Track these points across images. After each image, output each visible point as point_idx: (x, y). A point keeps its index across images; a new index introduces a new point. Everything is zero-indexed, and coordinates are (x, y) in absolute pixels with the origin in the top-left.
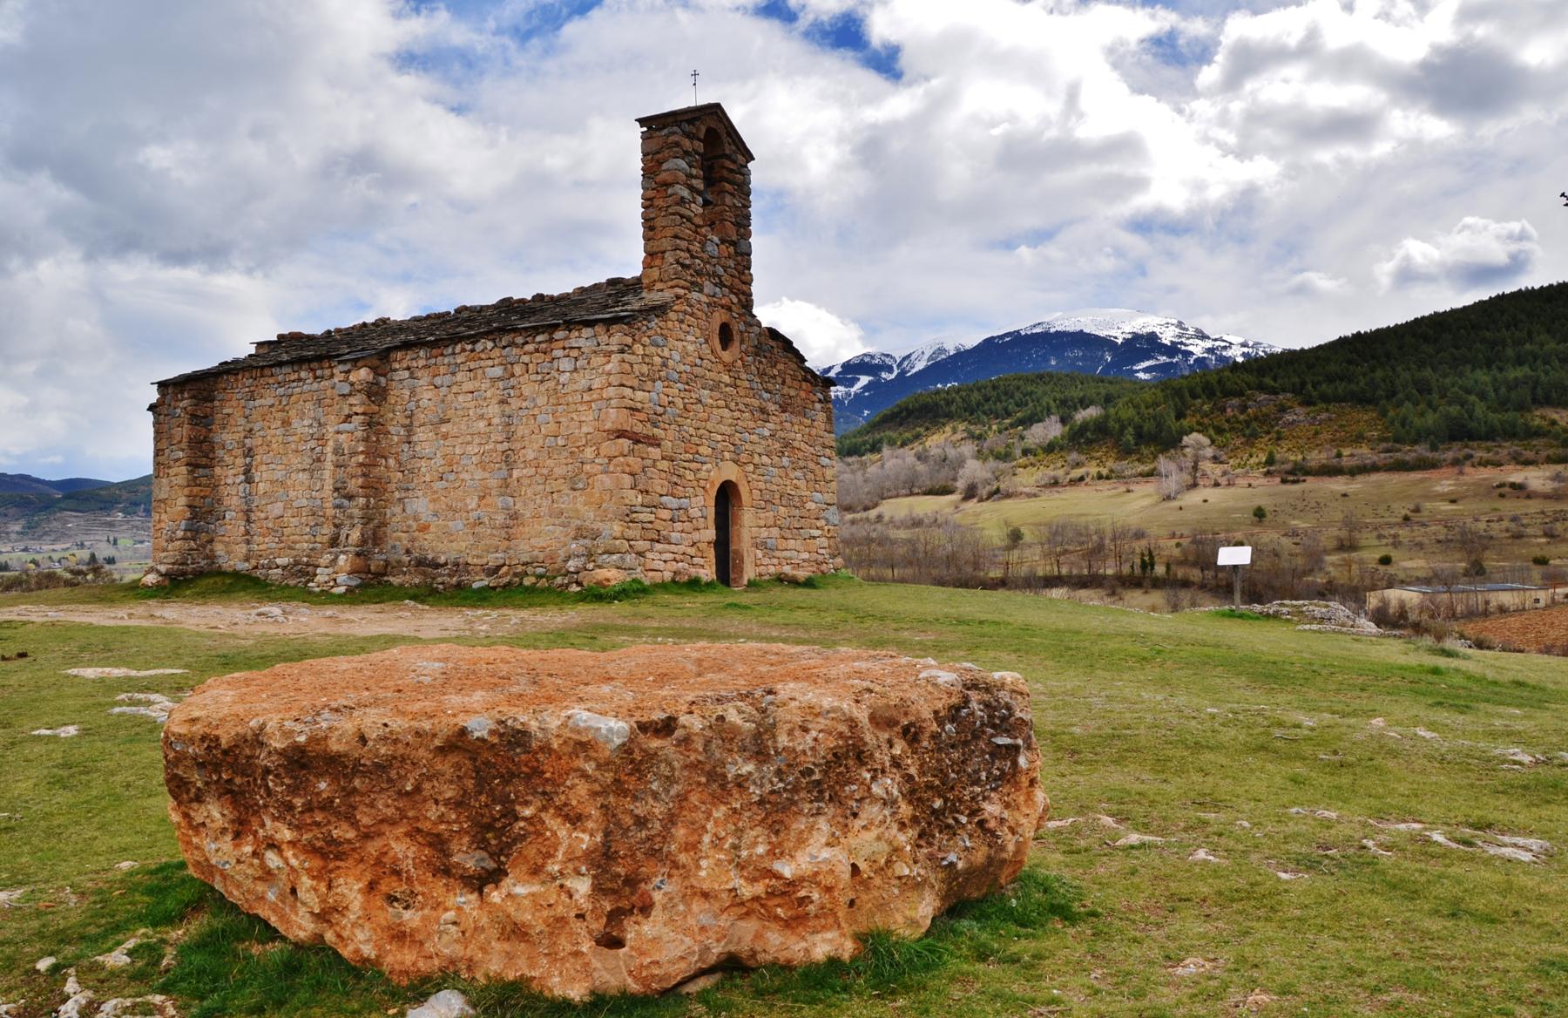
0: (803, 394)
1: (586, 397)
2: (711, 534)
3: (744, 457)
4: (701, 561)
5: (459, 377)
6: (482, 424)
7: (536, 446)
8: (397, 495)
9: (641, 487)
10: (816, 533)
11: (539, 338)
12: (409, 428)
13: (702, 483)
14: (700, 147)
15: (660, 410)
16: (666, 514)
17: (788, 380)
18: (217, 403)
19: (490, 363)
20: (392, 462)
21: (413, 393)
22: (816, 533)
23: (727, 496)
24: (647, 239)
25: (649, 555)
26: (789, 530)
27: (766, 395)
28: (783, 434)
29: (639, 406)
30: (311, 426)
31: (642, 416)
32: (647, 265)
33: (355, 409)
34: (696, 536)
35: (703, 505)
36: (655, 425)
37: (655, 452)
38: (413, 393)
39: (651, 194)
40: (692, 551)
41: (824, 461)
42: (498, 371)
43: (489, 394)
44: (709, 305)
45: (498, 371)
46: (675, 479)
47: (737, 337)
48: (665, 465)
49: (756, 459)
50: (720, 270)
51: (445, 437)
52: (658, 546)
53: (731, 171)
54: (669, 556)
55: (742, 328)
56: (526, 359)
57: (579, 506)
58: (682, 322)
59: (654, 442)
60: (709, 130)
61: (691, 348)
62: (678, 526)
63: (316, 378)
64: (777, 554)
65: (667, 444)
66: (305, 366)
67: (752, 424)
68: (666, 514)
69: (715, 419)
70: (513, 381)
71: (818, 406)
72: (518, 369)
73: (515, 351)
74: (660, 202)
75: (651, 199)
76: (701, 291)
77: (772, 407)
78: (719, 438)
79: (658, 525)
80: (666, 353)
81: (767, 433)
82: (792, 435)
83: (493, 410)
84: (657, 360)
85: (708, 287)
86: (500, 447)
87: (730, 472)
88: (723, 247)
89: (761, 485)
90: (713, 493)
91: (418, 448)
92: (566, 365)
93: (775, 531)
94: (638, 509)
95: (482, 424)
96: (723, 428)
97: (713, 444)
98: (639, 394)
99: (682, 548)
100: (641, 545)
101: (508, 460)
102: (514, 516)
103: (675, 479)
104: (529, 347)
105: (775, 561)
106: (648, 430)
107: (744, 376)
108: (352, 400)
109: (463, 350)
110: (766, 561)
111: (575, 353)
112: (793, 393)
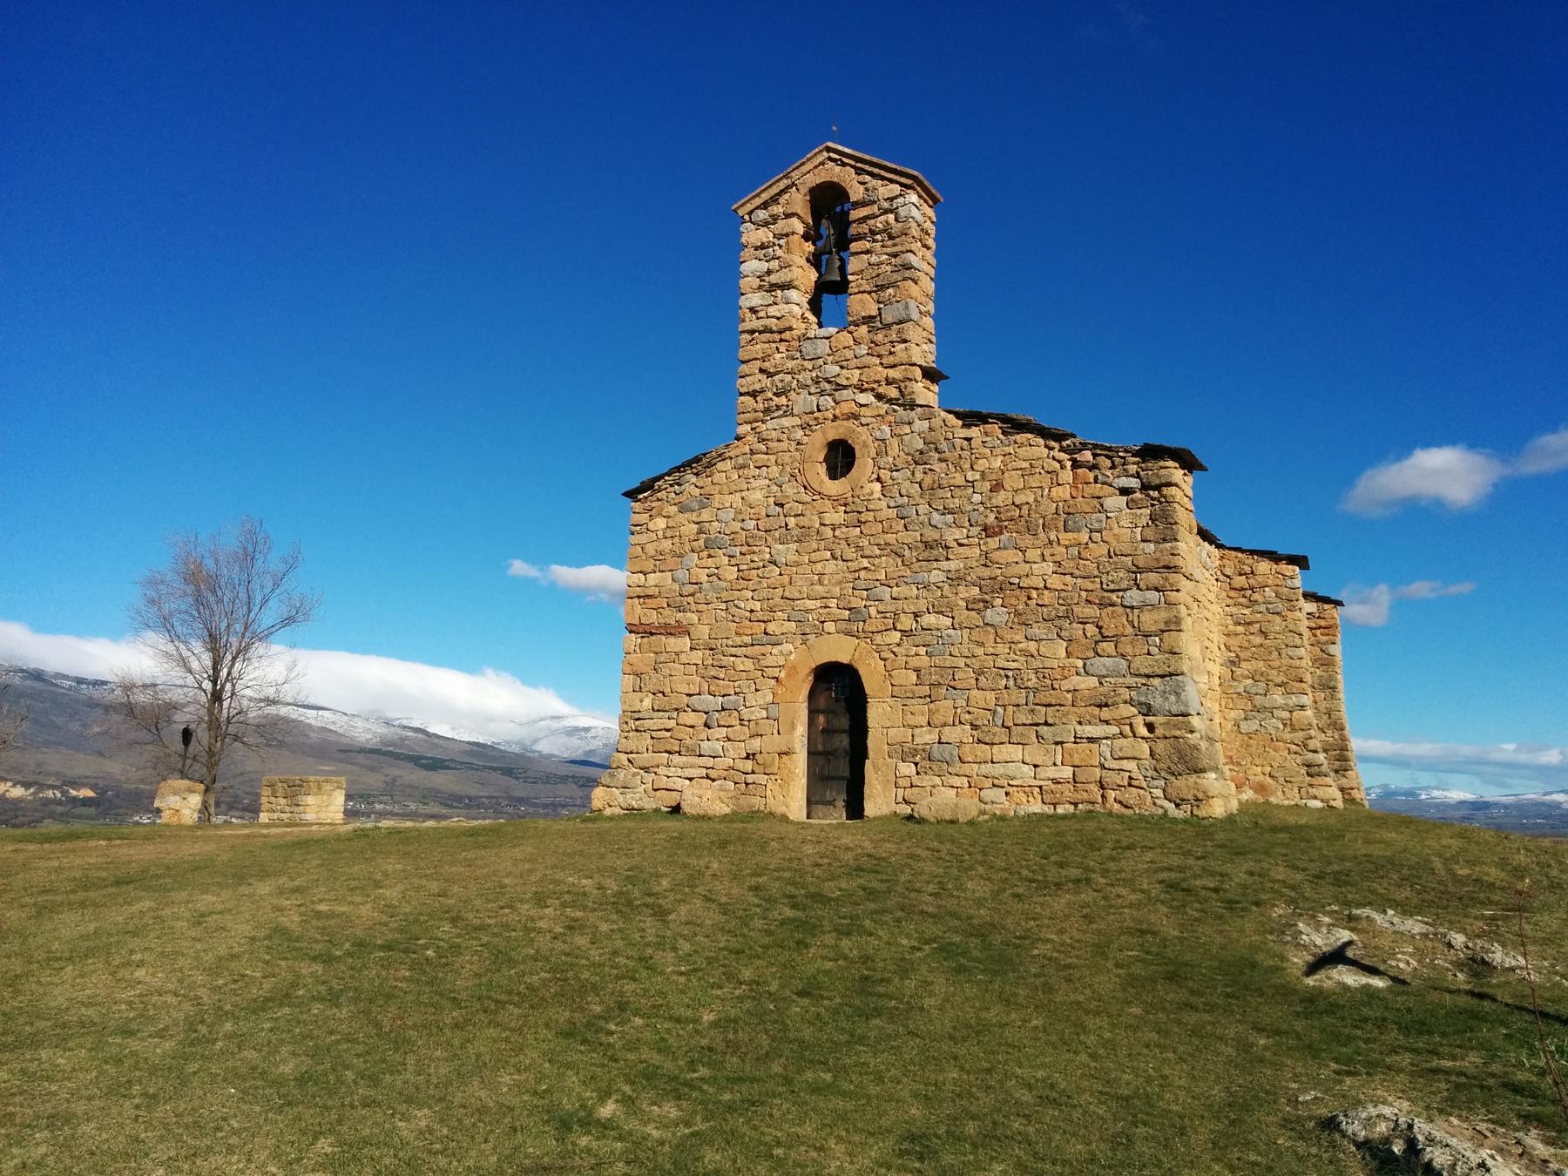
9: (652, 688)
16: (698, 719)
34: (756, 744)
36: (680, 609)
37: (674, 643)
49: (906, 622)
52: (676, 759)
58: (743, 467)
59: (679, 630)
61: (757, 496)
65: (703, 632)
76: (788, 413)
78: (810, 604)
87: (839, 650)
89: (924, 661)
106: (671, 617)
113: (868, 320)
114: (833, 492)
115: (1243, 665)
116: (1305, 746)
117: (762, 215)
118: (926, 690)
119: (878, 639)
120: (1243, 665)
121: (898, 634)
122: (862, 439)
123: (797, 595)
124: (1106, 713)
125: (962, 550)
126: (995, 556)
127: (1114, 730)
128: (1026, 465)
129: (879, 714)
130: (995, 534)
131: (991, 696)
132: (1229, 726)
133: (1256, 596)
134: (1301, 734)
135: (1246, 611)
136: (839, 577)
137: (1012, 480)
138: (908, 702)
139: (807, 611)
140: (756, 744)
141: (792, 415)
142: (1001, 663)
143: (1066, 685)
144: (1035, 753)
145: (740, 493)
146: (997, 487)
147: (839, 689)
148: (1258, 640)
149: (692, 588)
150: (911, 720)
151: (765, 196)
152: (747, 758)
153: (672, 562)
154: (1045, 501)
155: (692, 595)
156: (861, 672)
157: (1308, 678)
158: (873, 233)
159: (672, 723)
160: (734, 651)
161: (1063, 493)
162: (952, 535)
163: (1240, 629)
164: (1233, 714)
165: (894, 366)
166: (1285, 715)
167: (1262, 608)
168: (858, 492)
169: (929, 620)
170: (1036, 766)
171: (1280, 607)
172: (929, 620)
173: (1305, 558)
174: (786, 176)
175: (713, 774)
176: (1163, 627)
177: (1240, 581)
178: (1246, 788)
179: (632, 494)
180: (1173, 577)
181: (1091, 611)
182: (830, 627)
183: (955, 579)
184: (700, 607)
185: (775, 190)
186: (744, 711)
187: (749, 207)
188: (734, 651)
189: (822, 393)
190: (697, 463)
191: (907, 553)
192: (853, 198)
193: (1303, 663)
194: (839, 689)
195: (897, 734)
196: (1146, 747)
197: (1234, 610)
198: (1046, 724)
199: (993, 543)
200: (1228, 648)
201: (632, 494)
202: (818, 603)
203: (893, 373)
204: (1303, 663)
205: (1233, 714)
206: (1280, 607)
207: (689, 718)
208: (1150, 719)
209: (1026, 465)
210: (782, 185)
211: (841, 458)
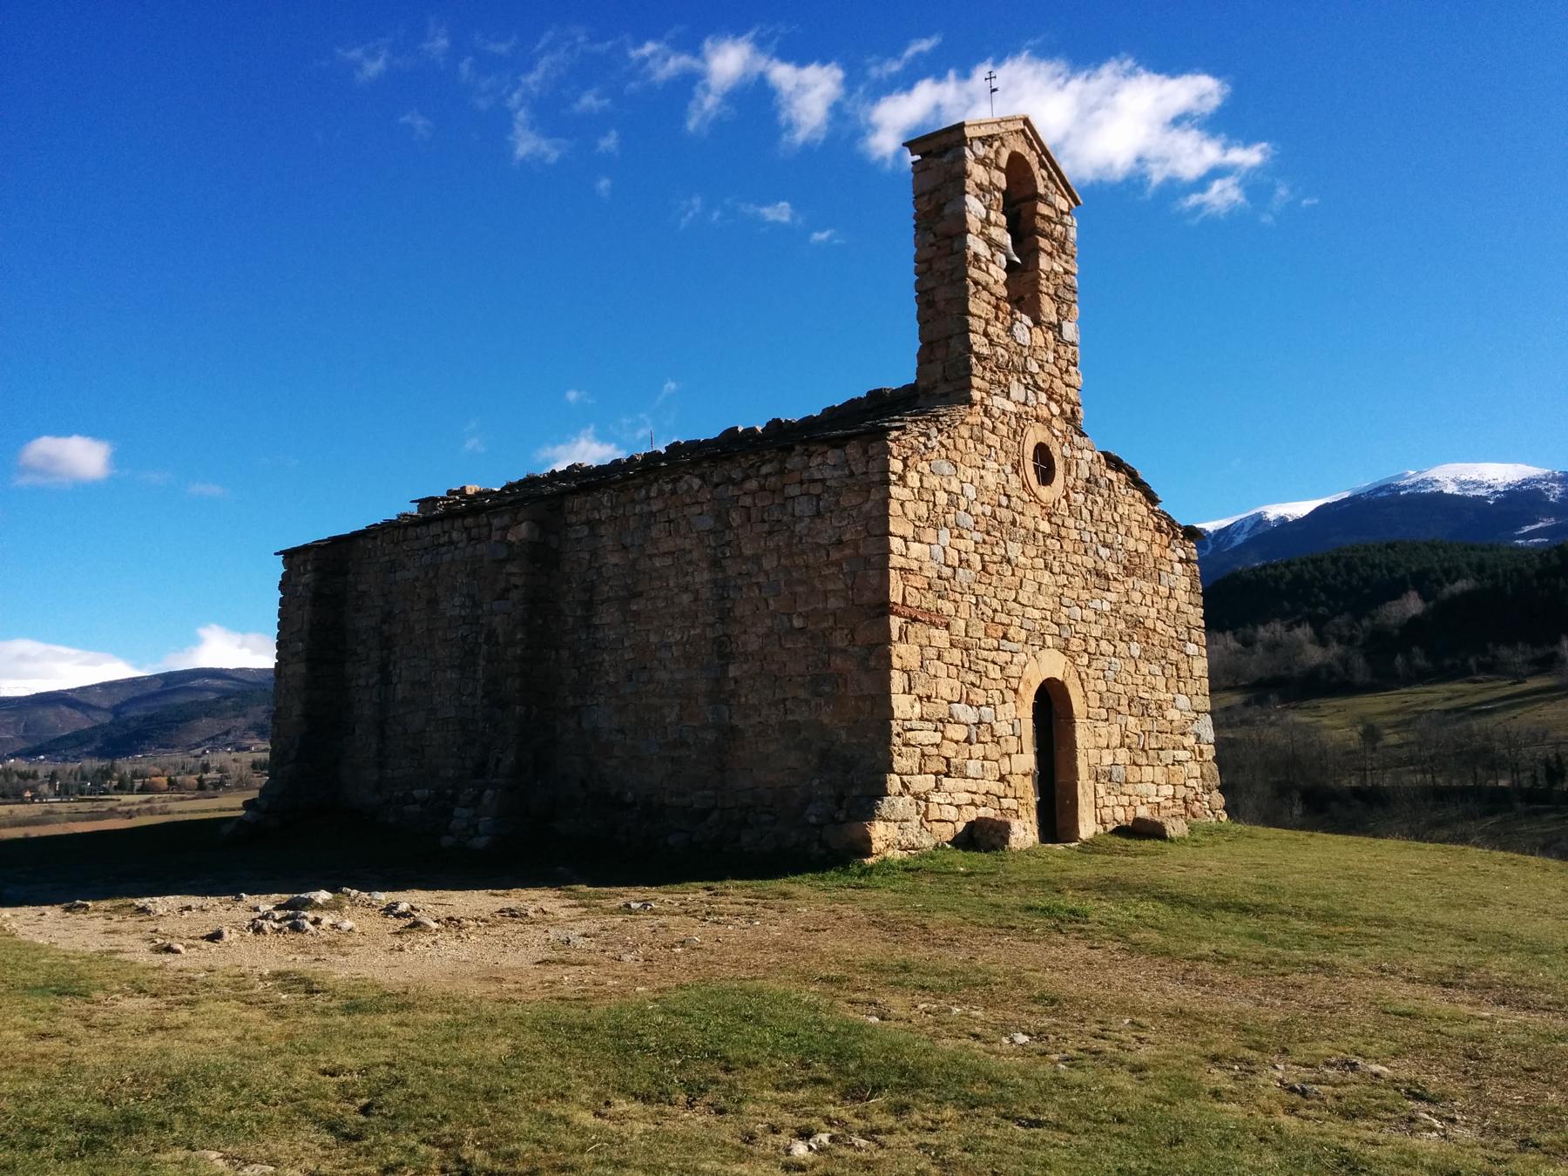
0: (1156, 550)
1: (835, 555)
2: (1028, 761)
3: (1076, 644)
4: (1013, 804)
5: (654, 533)
6: (686, 598)
7: (761, 630)
8: (571, 701)
9: (919, 690)
10: (1182, 755)
11: (765, 470)
12: (589, 606)
13: (1014, 683)
14: (1001, 180)
15: (947, 572)
16: (958, 733)
17: (1135, 531)
18: (350, 578)
19: (696, 509)
20: (565, 654)
21: (594, 553)
22: (1182, 755)
24: (923, 320)
25: (935, 798)
26: (1140, 752)
27: (1104, 552)
28: (1129, 609)
29: (915, 565)
30: (463, 606)
31: (918, 582)
32: (925, 357)
33: (514, 580)
34: (1005, 766)
35: (1018, 717)
37: (940, 637)
38: (594, 553)
39: (927, 254)
40: (998, 788)
41: (1192, 649)
42: (708, 523)
43: (695, 555)
44: (1018, 417)
45: (708, 523)
46: (971, 677)
47: (1059, 466)
48: (956, 656)
50: (1034, 368)
51: (637, 614)
53: (1048, 219)
54: (964, 798)
55: (1067, 451)
56: (747, 501)
57: (826, 721)
60: (1015, 158)
62: (977, 750)
63: (470, 539)
64: (1128, 789)
66: (458, 523)
67: (1085, 595)
68: (958, 733)
69: (1029, 587)
70: (729, 536)
71: (1178, 567)
72: (736, 518)
73: (732, 491)
74: (939, 265)
75: (929, 261)
77: (1111, 569)
78: (1037, 614)
79: (949, 750)
80: (955, 486)
81: (1106, 607)
82: (1143, 611)
83: (703, 576)
84: (942, 498)
85: (1017, 392)
86: (709, 634)
87: (1052, 665)
88: (1036, 331)
89: (1101, 686)
90: (1030, 699)
91: (599, 635)
92: (803, 507)
93: (1123, 755)
94: (916, 724)
95: (686, 598)
96: (1042, 601)
97: (1028, 624)
98: (914, 546)
99: (984, 786)
100: (923, 783)
101: (724, 651)
102: (731, 733)
103: (971, 677)
104: (752, 485)
105: (1125, 800)
106: (930, 601)
107: (1070, 522)
108: (511, 568)
109: (661, 493)
110: (1111, 800)
111: (816, 489)
112: (1142, 548)
113: (1051, 326)
129: (1082, 735)
147: (1052, 707)
153: (929, 535)
159: (937, 737)
175: (978, 799)
184: (958, 597)
186: (996, 726)
194: (1052, 707)
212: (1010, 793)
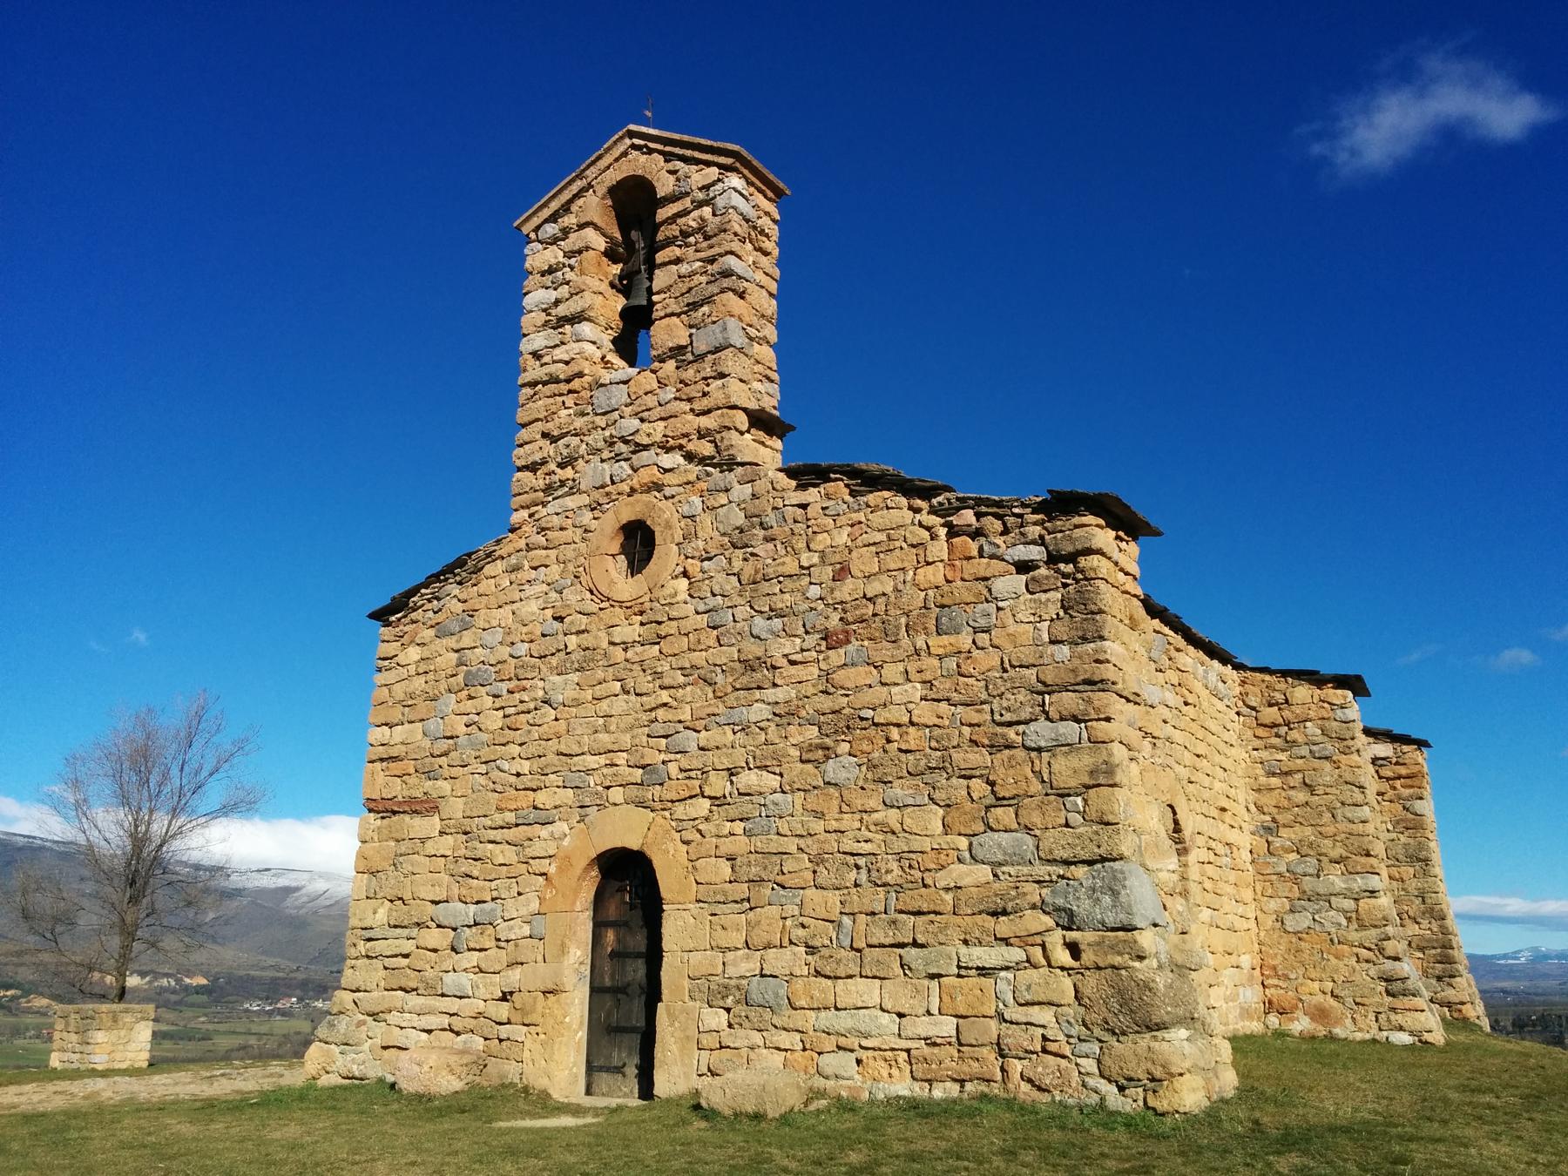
9: (390, 893)
13: (537, 865)
23: (627, 881)
34: (515, 977)
36: (430, 775)
40: (503, 1010)
49: (718, 784)
52: (413, 1001)
58: (516, 569)
59: (425, 806)
65: (455, 808)
78: (592, 761)
87: (626, 829)
89: (740, 845)
103: (465, 867)
106: (419, 787)
114: (625, 596)
115: (1283, 832)
116: (1381, 950)
117: (551, 229)
118: (742, 890)
119: (680, 810)
120: (1283, 832)
121: (707, 803)
122: (664, 516)
123: (576, 749)
124: (1004, 926)
125: (793, 670)
126: (839, 677)
127: (1017, 954)
128: (881, 537)
129: (677, 928)
130: (840, 644)
131: (834, 898)
132: (1269, 921)
133: (1294, 735)
134: (1374, 932)
135: (1282, 756)
136: (630, 719)
137: (863, 561)
138: (719, 909)
139: (589, 772)
140: (515, 977)
141: (580, 492)
142: (849, 845)
143: (943, 879)
144: (899, 993)
145: (508, 606)
146: (842, 572)
148: (1301, 796)
149: (444, 745)
150: (724, 939)
151: (555, 205)
152: (504, 998)
153: (423, 708)
154: (909, 589)
155: (445, 754)
156: (657, 864)
157: (1379, 848)
158: (685, 234)
159: (408, 946)
160: (492, 834)
161: (935, 574)
162: (781, 648)
163: (1275, 781)
164: (1273, 905)
165: (708, 412)
166: (1349, 904)
167: (1304, 751)
168: (657, 593)
169: (749, 779)
170: (901, 1015)
171: (1329, 748)
172: (749, 779)
173: (1359, 678)
174: (579, 177)
175: (457, 1024)
176: (1087, 780)
177: (1271, 714)
178: (1299, 1013)
179: (381, 616)
180: (1099, 698)
181: (978, 758)
182: (617, 794)
183: (785, 715)
185: (566, 196)
187: (536, 221)
188: (492, 834)
189: (617, 458)
190: (460, 568)
191: (720, 679)
192: (661, 193)
193: (1370, 828)
195: (703, 961)
196: (1067, 983)
197: (1264, 754)
198: (915, 944)
199: (837, 657)
200: (1260, 809)
201: (381, 616)
202: (602, 760)
203: (707, 422)
204: (1370, 828)
205: (1273, 905)
206: (1329, 748)
207: (433, 937)
208: (1073, 935)
209: (881, 537)
210: (575, 188)
211: (638, 543)
212: (516, 1018)
